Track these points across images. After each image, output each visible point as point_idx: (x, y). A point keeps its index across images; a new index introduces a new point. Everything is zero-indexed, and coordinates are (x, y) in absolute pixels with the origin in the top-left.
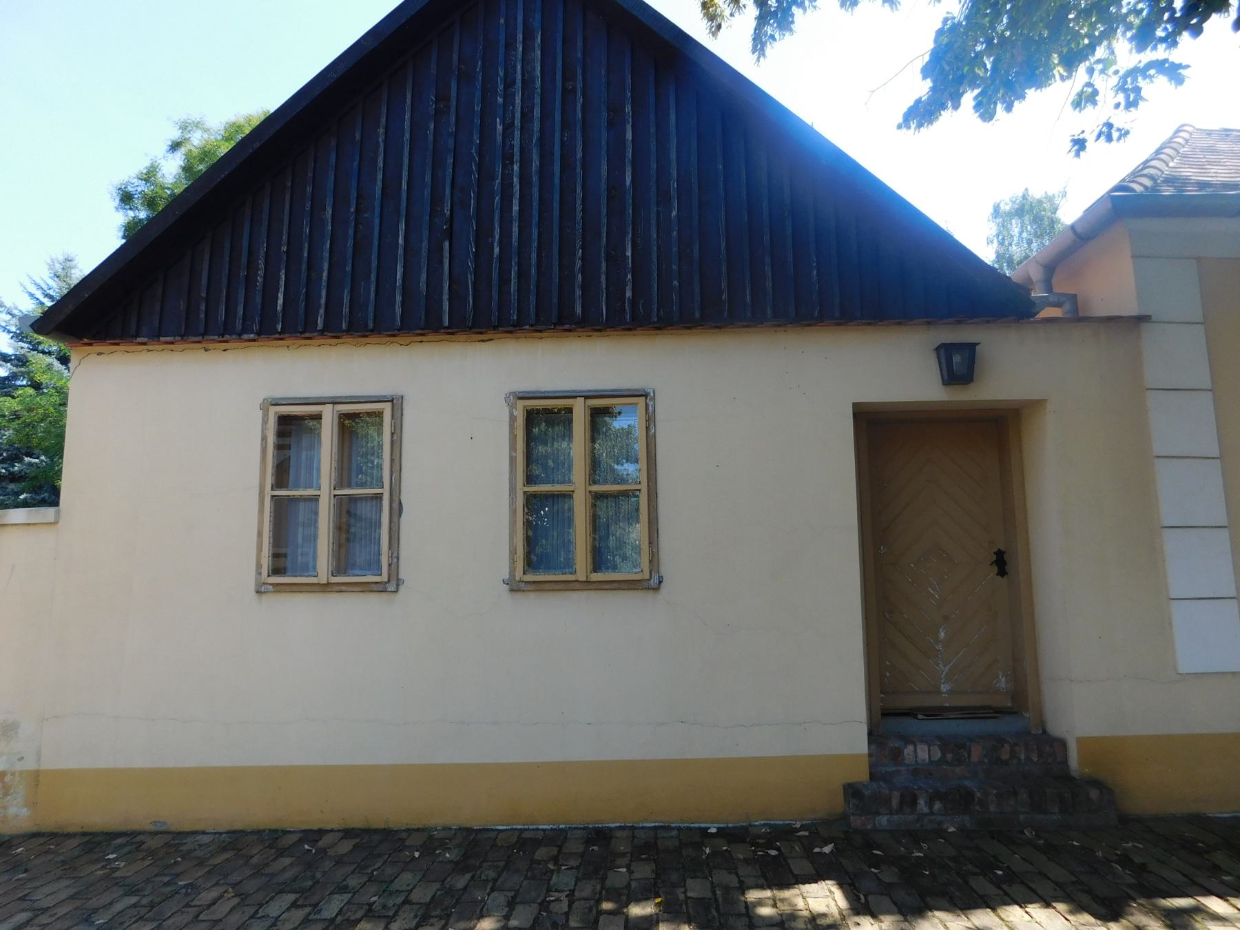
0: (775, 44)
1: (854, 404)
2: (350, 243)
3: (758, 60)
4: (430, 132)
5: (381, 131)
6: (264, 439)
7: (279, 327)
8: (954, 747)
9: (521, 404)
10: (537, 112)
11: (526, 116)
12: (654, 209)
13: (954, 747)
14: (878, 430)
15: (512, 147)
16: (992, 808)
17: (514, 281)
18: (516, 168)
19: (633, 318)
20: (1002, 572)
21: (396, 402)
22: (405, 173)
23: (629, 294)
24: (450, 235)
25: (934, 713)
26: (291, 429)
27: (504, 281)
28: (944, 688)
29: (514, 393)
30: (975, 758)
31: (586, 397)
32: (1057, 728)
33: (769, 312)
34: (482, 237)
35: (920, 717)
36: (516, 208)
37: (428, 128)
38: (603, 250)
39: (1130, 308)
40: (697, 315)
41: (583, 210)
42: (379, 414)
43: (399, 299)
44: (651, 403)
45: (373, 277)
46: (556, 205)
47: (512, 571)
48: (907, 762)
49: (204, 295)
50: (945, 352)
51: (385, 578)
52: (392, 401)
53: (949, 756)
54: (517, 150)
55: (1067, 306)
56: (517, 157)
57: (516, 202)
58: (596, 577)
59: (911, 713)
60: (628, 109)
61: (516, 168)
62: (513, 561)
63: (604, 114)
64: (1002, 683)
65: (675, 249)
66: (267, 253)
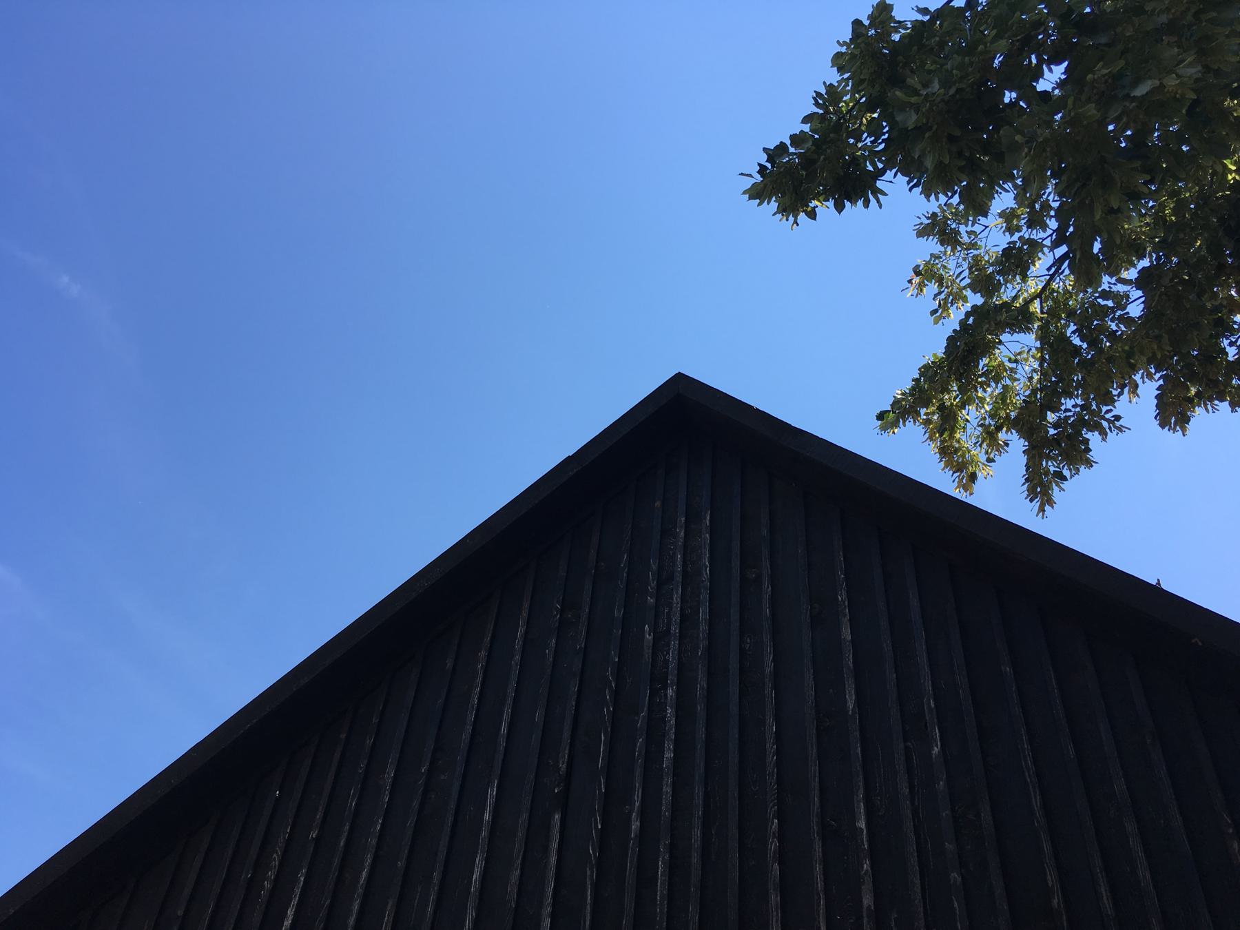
0: (1065, 485)
3: (1042, 509)
5: (483, 654)
11: (687, 620)
15: (666, 662)
23: (868, 900)
36: (669, 755)
41: (778, 752)
43: (470, 915)
49: (180, 913)
54: (672, 666)
56: (672, 678)
57: (669, 746)
65: (946, 813)
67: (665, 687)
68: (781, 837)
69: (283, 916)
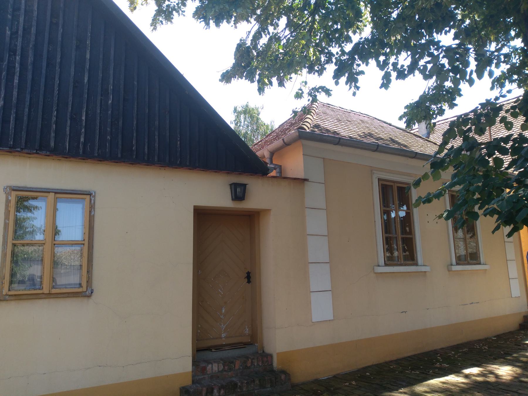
1: (194, 206)
8: (228, 363)
9: (14, 194)
10: (33, 30)
12: (99, 98)
13: (228, 363)
14: (203, 216)
15: (16, 46)
16: (244, 389)
18: (18, 58)
19: (84, 152)
20: (249, 282)
23: (82, 140)
25: (219, 348)
28: (223, 335)
29: (10, 187)
30: (237, 368)
31: (56, 193)
32: (268, 350)
33: (156, 158)
35: (213, 350)
36: (16, 81)
38: (69, 114)
39: (301, 175)
40: (119, 156)
41: (59, 90)
44: (93, 199)
48: (208, 373)
50: (234, 187)
53: (226, 368)
55: (278, 170)
56: (19, 52)
58: (54, 291)
59: (209, 349)
61: (18, 58)
64: (247, 331)
65: (109, 120)
67: (15, 55)
68: (57, 117)
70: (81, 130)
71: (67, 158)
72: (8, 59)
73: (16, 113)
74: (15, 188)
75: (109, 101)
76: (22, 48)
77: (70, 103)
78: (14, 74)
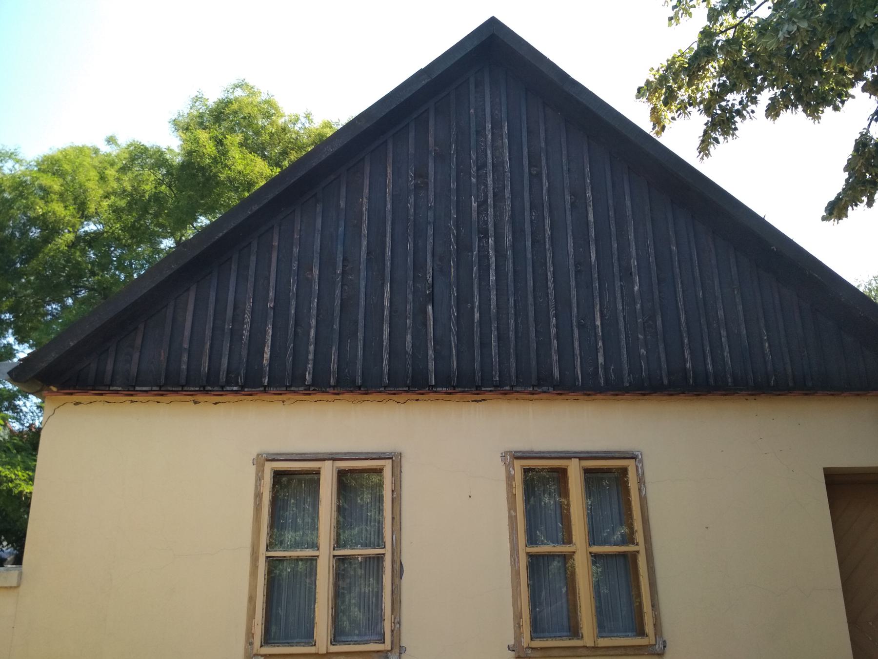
0: (717, 146)
2: (338, 302)
4: (411, 206)
6: (258, 496)
7: (266, 381)
9: (518, 464)
10: (507, 193)
11: (498, 196)
12: (618, 284)
15: (486, 223)
17: (494, 344)
18: (491, 241)
19: (607, 380)
21: (395, 458)
22: (388, 241)
23: (601, 360)
24: (432, 298)
26: (289, 487)
27: (485, 344)
34: (463, 300)
36: (493, 278)
37: (408, 202)
41: (554, 282)
42: (379, 471)
43: (386, 357)
44: (640, 465)
45: (360, 335)
46: (530, 277)
47: (518, 635)
49: (186, 346)
51: (387, 645)
52: (391, 458)
56: (491, 232)
57: (492, 273)
60: (589, 194)
61: (491, 241)
62: (518, 626)
63: (568, 197)
66: (253, 308)
67: (486, 236)
68: (557, 327)
69: (263, 352)
70: (597, 344)
71: (589, 395)
72: (479, 246)
73: (498, 329)
74: (519, 454)
75: (634, 287)
76: (495, 225)
77: (574, 301)
78: (488, 266)
